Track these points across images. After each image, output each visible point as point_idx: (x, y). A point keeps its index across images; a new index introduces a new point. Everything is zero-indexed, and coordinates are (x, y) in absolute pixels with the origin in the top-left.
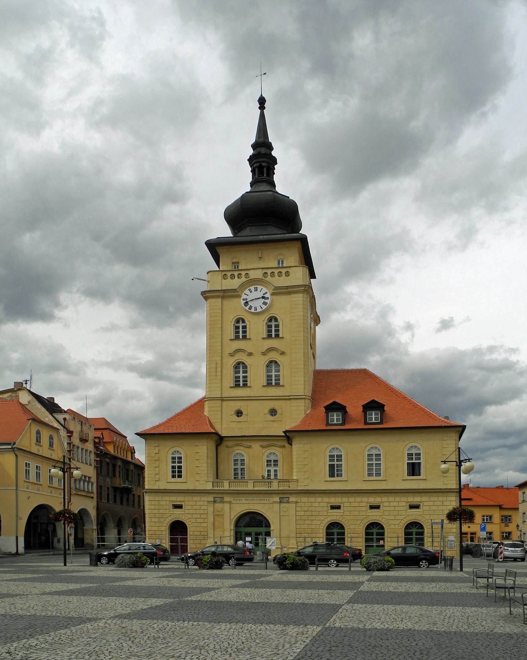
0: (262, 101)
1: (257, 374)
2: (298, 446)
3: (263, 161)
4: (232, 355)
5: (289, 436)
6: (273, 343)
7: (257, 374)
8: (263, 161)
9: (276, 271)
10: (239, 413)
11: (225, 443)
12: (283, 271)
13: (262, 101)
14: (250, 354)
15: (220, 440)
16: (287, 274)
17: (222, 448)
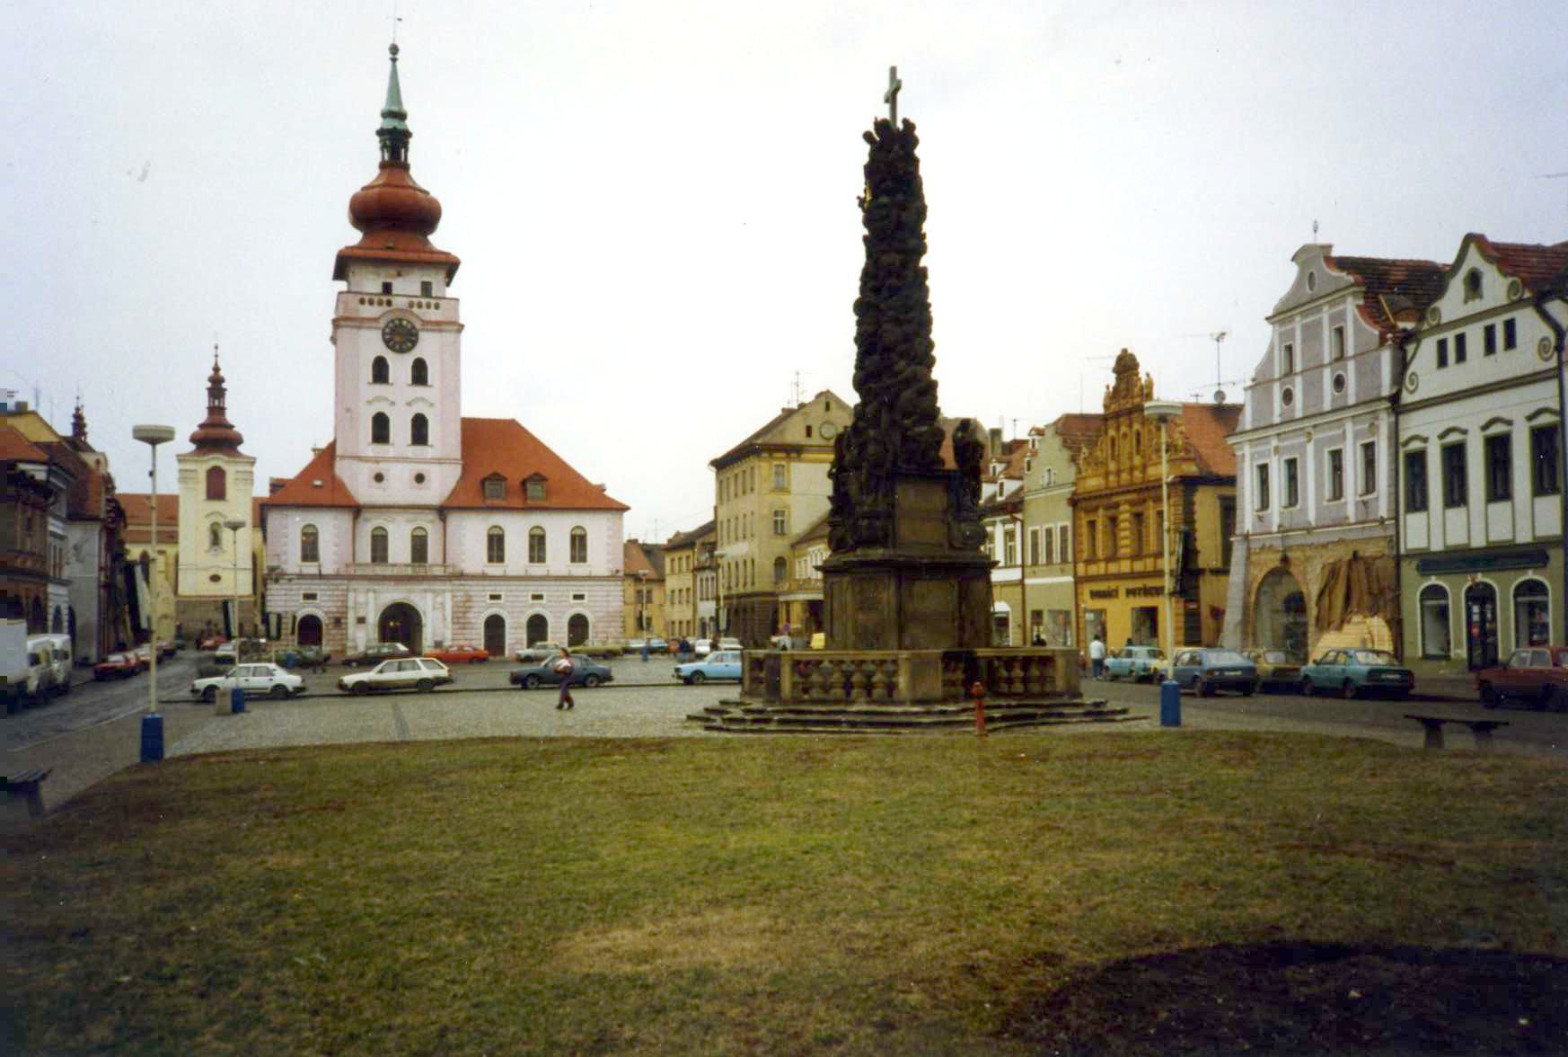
0: (394, 50)
1: (400, 430)
2: (454, 520)
3: (395, 140)
4: (369, 402)
5: (442, 511)
6: (420, 391)
7: (400, 430)
8: (395, 140)
9: (424, 301)
10: (379, 478)
11: (365, 515)
12: (433, 302)
13: (394, 50)
14: (393, 403)
15: (357, 510)
16: (437, 307)
17: (361, 520)
